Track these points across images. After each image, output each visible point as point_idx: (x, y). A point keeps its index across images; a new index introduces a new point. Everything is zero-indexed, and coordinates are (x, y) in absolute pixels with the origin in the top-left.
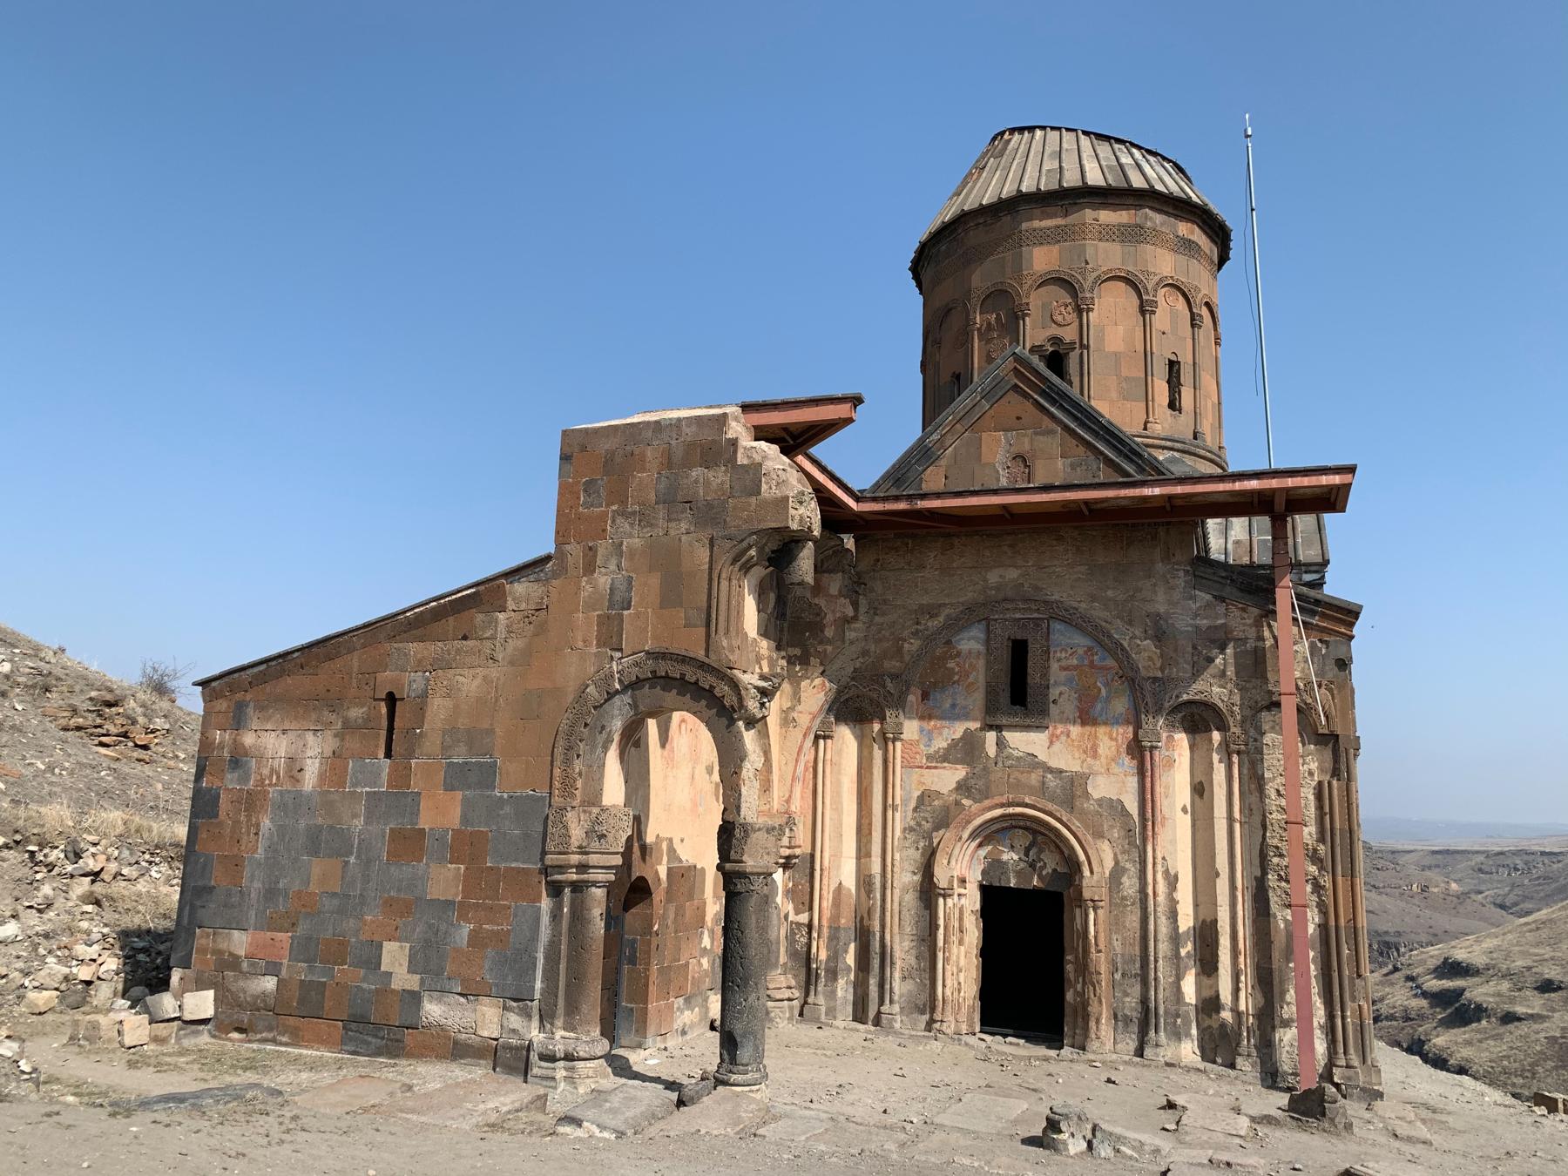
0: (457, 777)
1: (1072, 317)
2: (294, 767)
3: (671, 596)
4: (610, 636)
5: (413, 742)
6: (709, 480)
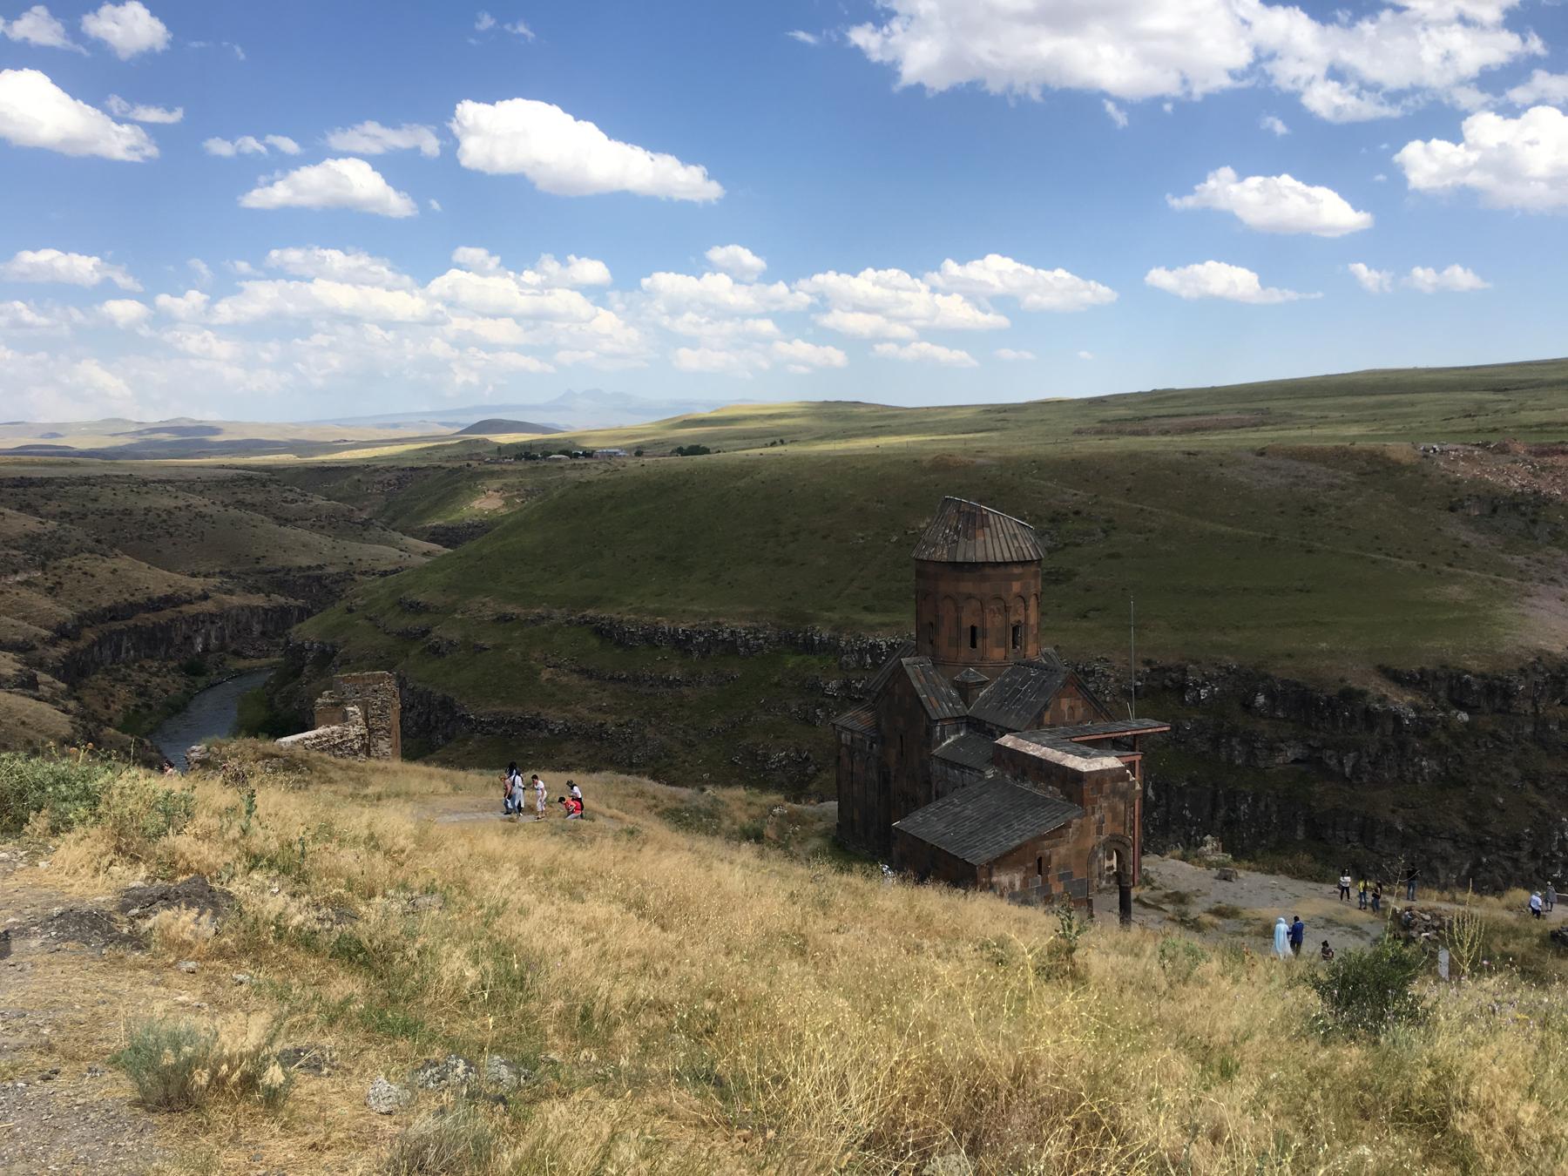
0: (1061, 878)
1: (1022, 610)
2: (1012, 885)
3: (1114, 818)
4: (1099, 832)
5: (1048, 871)
6: (1123, 785)
